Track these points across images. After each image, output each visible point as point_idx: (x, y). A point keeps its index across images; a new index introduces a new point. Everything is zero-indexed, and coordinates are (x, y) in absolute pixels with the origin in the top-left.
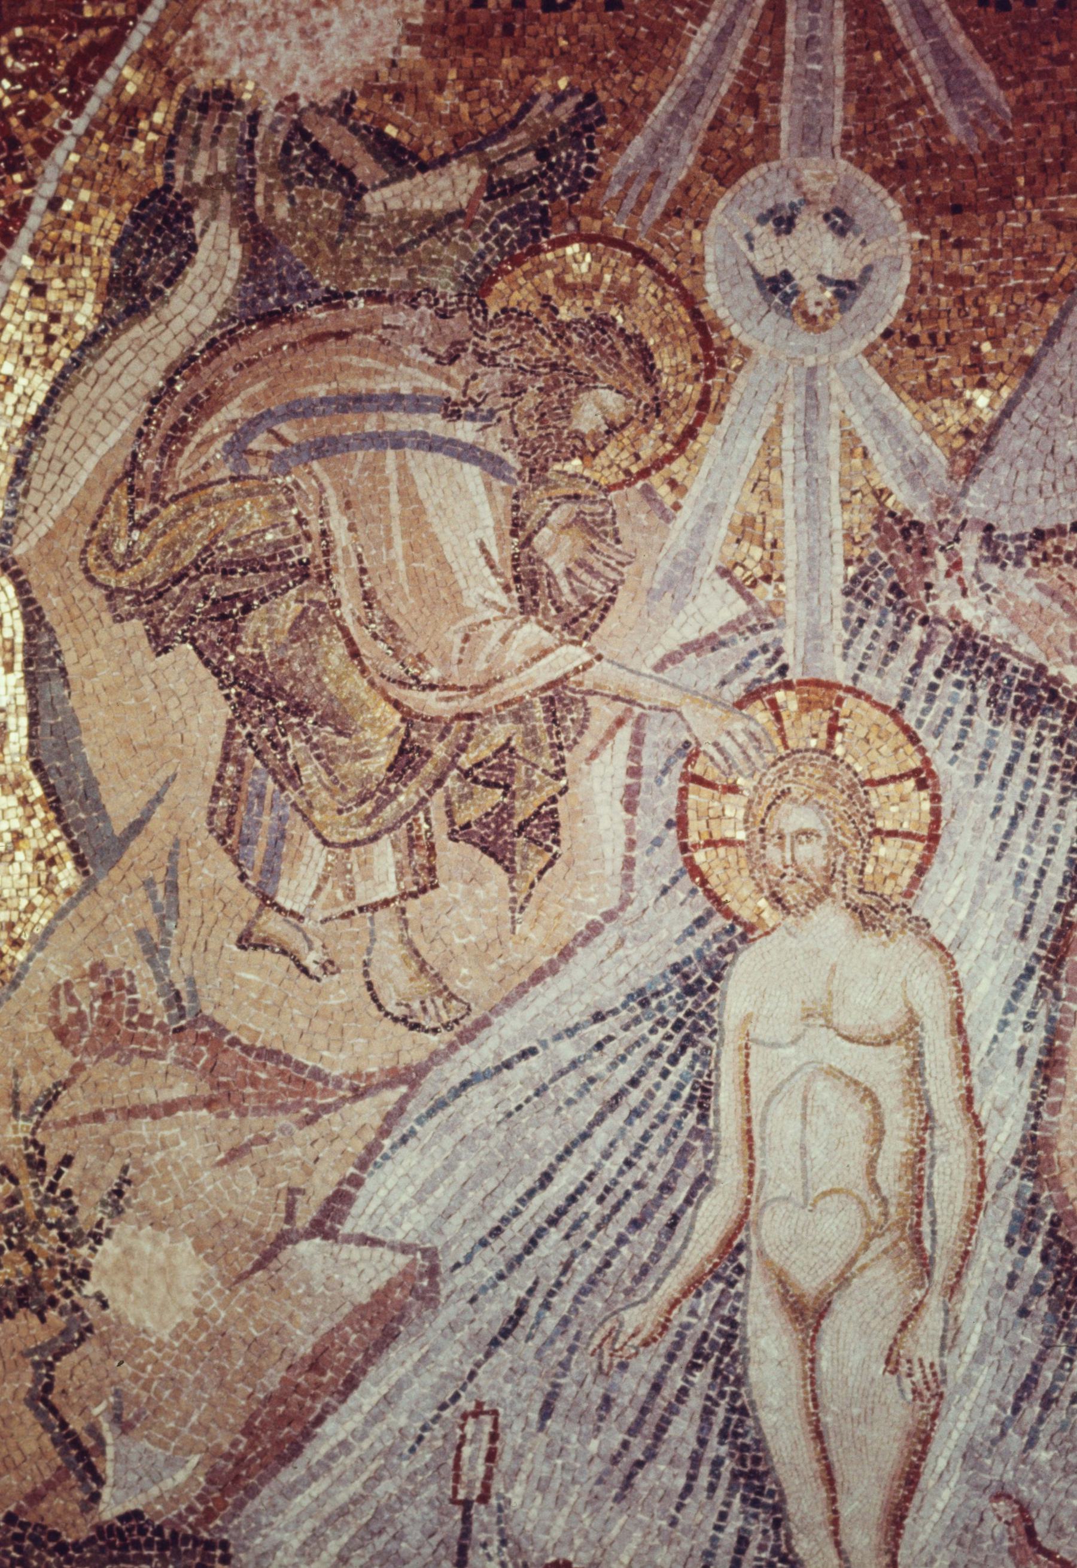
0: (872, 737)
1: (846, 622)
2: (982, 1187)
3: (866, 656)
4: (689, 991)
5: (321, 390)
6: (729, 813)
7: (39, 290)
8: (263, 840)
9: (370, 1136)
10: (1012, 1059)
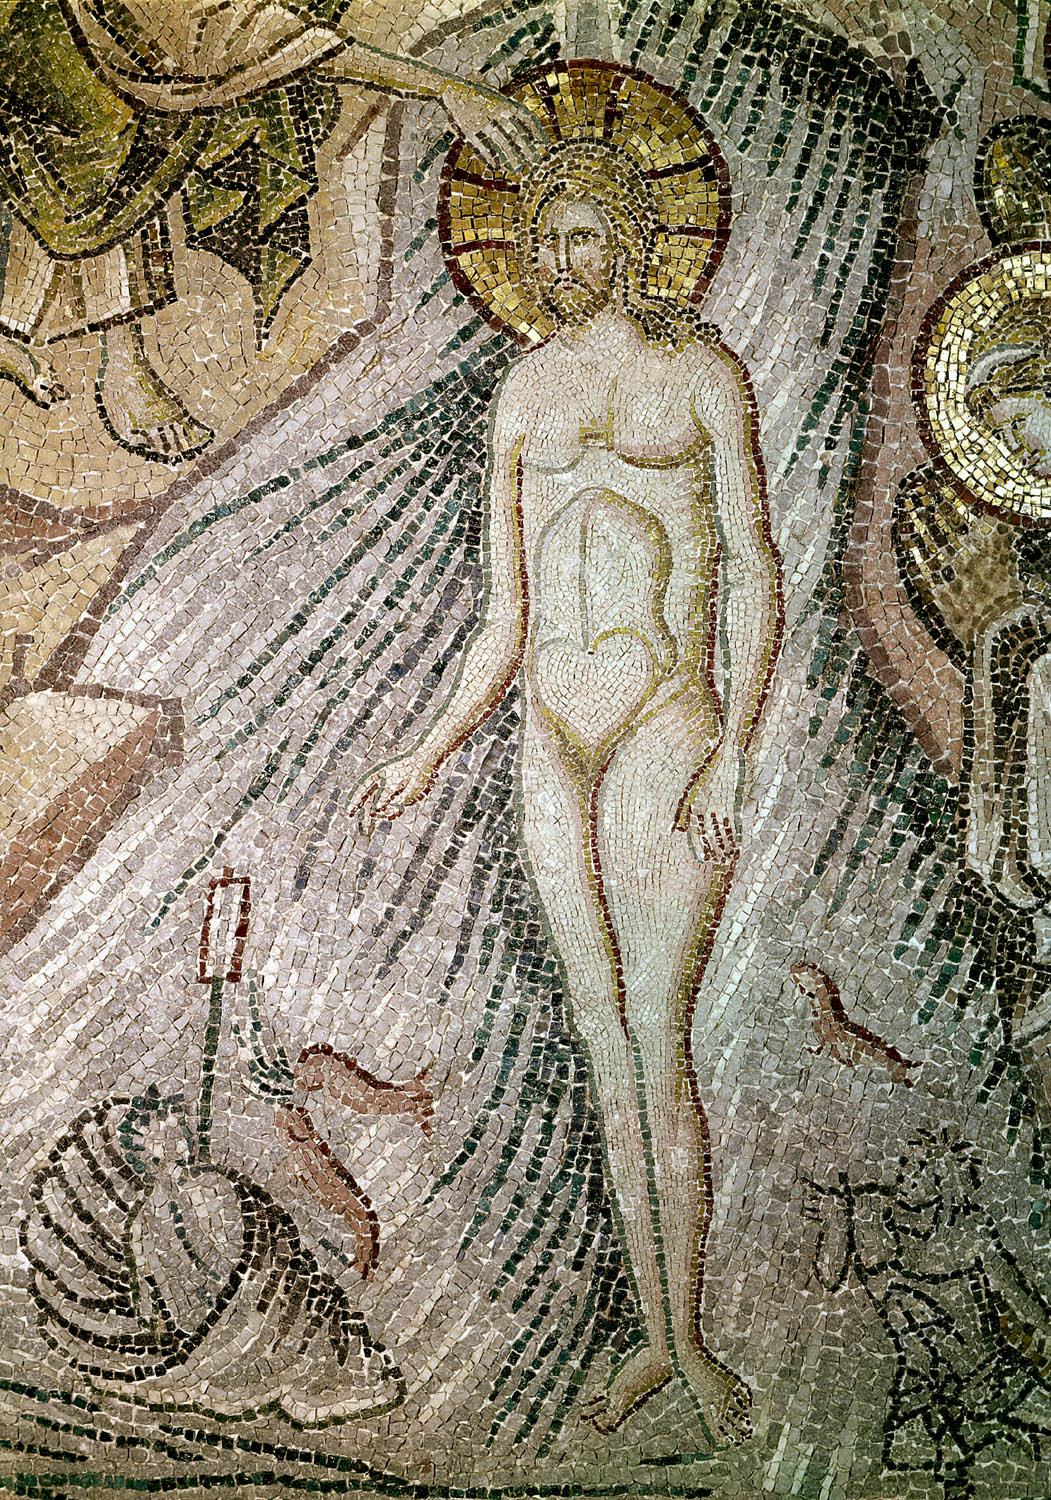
2: (781, 622)
3: (645, 34)
9: (105, 577)
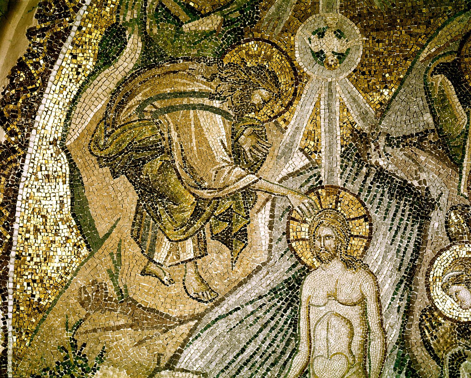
0: (350, 204)
1: (341, 166)
2: (386, 352)
4: (290, 288)
5: (168, 90)
6: (303, 230)
7: (74, 57)
8: (149, 240)
9: (185, 337)
10: (396, 309)
